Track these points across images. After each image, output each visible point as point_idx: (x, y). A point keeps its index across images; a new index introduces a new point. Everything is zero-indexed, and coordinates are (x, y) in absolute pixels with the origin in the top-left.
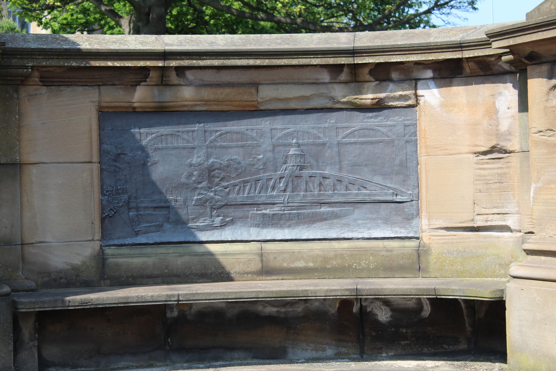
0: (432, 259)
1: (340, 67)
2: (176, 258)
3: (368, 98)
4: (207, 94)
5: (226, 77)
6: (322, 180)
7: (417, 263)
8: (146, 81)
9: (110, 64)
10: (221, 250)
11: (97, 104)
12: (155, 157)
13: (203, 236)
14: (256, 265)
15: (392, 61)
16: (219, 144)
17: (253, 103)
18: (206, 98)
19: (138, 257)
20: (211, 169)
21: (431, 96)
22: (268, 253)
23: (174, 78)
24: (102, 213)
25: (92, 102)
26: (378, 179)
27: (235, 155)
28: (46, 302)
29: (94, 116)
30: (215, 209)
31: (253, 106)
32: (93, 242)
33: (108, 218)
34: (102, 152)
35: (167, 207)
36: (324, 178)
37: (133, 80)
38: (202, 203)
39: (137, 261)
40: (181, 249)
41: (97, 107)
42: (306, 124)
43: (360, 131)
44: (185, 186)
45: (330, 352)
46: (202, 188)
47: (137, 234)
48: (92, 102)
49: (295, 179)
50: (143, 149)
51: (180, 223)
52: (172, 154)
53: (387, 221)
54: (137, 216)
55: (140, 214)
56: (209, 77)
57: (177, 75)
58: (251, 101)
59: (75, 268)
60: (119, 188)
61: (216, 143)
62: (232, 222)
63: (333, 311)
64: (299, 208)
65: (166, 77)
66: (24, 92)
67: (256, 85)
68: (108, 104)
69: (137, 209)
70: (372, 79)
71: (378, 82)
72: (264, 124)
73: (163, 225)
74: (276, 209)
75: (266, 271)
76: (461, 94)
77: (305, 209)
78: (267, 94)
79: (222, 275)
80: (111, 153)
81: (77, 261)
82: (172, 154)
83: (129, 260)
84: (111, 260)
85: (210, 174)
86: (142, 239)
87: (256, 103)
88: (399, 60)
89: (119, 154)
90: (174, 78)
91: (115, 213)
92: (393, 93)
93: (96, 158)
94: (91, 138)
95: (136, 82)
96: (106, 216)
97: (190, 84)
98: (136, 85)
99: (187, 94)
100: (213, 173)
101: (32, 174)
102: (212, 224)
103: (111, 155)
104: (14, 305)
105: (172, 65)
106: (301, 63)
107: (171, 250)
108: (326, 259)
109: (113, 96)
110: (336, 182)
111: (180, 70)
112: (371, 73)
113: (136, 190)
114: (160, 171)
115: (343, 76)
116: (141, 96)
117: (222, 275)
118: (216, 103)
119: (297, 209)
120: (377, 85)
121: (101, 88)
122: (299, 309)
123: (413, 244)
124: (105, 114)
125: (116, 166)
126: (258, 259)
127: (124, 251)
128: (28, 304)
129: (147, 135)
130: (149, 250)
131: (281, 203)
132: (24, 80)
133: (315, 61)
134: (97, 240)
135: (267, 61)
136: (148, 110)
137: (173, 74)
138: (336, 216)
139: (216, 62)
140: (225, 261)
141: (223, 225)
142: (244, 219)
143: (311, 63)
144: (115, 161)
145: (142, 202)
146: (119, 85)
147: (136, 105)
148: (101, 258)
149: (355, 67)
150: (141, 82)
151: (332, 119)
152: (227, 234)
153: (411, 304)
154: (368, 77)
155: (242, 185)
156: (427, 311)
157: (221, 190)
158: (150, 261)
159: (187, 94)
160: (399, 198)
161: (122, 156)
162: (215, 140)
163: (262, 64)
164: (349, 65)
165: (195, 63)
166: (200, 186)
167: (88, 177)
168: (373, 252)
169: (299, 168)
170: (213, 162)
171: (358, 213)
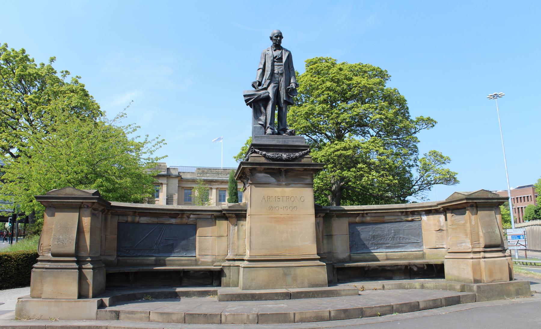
0: (426, 256)
1: (403, 212)
2: (367, 256)
3: (410, 219)
4: (372, 219)
5: (377, 215)
7: (423, 256)
12: (361, 233)
13: (373, 251)
14: (385, 258)
20: (374, 236)
21: (424, 218)
23: (365, 215)
26: (413, 237)
27: (379, 232)
28: (340, 265)
29: (348, 224)
33: (351, 247)
34: (349, 232)
35: (364, 244)
38: (372, 244)
39: (358, 257)
40: (368, 254)
42: (396, 225)
44: (368, 240)
45: (403, 278)
50: (358, 231)
51: (367, 248)
52: (365, 232)
53: (415, 247)
56: (373, 215)
59: (344, 258)
63: (403, 268)
66: (333, 219)
67: (384, 216)
72: (386, 225)
74: (389, 245)
75: (387, 259)
76: (431, 217)
78: (387, 218)
79: (378, 260)
81: (345, 257)
82: (365, 232)
85: (374, 237)
86: (359, 252)
90: (365, 215)
92: (416, 217)
99: (368, 219)
101: (335, 237)
104: (333, 266)
107: (366, 254)
108: (401, 256)
109: (352, 220)
111: (367, 214)
114: (362, 237)
115: (404, 214)
116: (358, 219)
117: (378, 260)
122: (396, 268)
123: (422, 252)
124: (350, 224)
128: (336, 266)
129: (359, 228)
132: (333, 216)
138: (403, 246)
140: (378, 257)
141: (377, 249)
142: (382, 247)
148: (350, 256)
149: (407, 212)
151: (402, 224)
152: (378, 251)
153: (422, 266)
156: (426, 268)
158: (361, 257)
159: (368, 219)
167: (347, 238)
168: (413, 254)
171: (408, 245)
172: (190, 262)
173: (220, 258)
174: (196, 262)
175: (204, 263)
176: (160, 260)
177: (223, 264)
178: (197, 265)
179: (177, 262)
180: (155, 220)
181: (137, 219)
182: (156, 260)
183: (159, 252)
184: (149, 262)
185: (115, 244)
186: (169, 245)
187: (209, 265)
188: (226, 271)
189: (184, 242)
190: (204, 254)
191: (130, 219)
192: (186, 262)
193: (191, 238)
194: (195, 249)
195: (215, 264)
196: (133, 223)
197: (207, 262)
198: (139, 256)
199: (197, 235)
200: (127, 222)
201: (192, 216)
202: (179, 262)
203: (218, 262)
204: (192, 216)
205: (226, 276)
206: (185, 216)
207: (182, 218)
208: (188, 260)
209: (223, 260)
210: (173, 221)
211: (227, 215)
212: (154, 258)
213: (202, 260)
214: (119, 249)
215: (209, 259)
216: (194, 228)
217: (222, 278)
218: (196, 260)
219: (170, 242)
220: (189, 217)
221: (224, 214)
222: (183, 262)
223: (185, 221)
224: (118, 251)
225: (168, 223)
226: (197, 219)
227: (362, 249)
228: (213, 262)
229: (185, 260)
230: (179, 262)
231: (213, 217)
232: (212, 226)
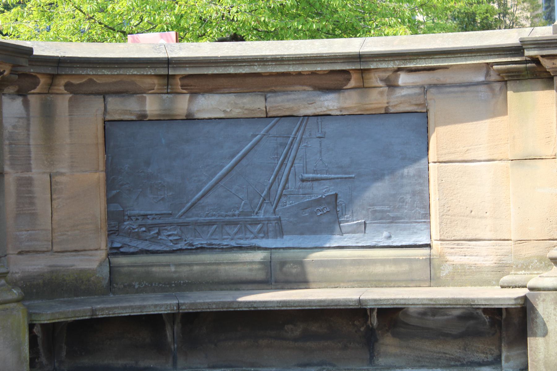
172: (405, 267)
173: (530, 251)
174: (431, 274)
175: (462, 275)
176: (283, 263)
177: (534, 282)
178: (432, 280)
179: (353, 271)
180: (254, 104)
181: (182, 104)
182: (267, 264)
183: (280, 232)
184: (242, 271)
185: (98, 207)
186: (319, 202)
187: (487, 283)
188: (544, 308)
189: (378, 190)
190: (461, 233)
191: (152, 106)
192: (389, 269)
193: (410, 170)
194: (427, 215)
195: (506, 279)
196: (167, 119)
197: (478, 269)
198: (202, 249)
199: (432, 155)
200: (142, 118)
201: (403, 79)
202: (362, 270)
203: (518, 268)
204: (403, 79)
205: (545, 334)
206: (375, 80)
207: (363, 87)
208: (396, 261)
209: (541, 259)
210: (330, 103)
211: (547, 64)
212: (259, 256)
213: (456, 259)
214: (115, 223)
215: (483, 256)
216: (419, 123)
217: (531, 341)
218: (430, 260)
219: (323, 190)
220: (392, 85)
221: (535, 60)
222: (379, 269)
223: (377, 99)
224: (112, 233)
225: (310, 111)
226: (425, 89)
228: (502, 268)
229: (384, 262)
230: (362, 270)
231: (494, 77)
232: (494, 114)
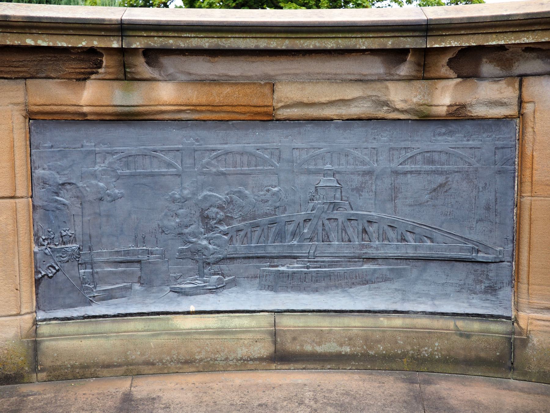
6: (366, 225)
8: (97, 73)
9: (30, 42)
10: (216, 326)
11: (22, 107)
14: (264, 349)
15: (490, 43)
16: (214, 170)
17: (265, 109)
18: (194, 101)
19: (90, 338)
22: (284, 331)
23: (143, 68)
24: (37, 272)
25: (15, 104)
30: (209, 264)
31: (266, 114)
32: (19, 317)
36: (369, 222)
37: (77, 70)
40: (156, 324)
41: (24, 113)
43: (426, 154)
46: (190, 234)
47: (89, 303)
48: (15, 104)
49: (327, 222)
54: (92, 274)
55: (97, 273)
57: (148, 63)
58: (264, 106)
60: (64, 234)
61: (211, 168)
62: (234, 283)
64: (331, 264)
65: (130, 68)
68: (40, 108)
69: (92, 264)
70: (451, 73)
71: (459, 80)
73: (131, 288)
74: (295, 266)
77: (340, 266)
80: (51, 183)
83: (76, 343)
84: (48, 345)
87: (271, 109)
88: (502, 42)
89: (63, 184)
91: (58, 271)
93: (22, 190)
94: (13, 161)
95: (83, 73)
96: (43, 276)
97: (170, 78)
98: (85, 79)
100: (206, 212)
102: (205, 286)
103: (50, 186)
105: (134, 46)
106: (341, 47)
110: (386, 227)
112: (450, 63)
113: (90, 238)
115: (404, 70)
118: (210, 108)
119: (329, 266)
120: (457, 84)
121: (29, 82)
125: (56, 201)
126: (269, 339)
127: (70, 328)
130: (107, 326)
131: (305, 257)
133: (364, 44)
134: (28, 313)
135: (287, 42)
136: (108, 118)
137: (141, 60)
139: (206, 43)
143: (358, 47)
144: (57, 194)
145: (100, 254)
146: (58, 78)
147: (85, 109)
150: (92, 73)
154: (445, 71)
155: (249, 230)
157: (217, 238)
160: (481, 256)
161: (68, 187)
162: (208, 163)
163: (279, 48)
164: (416, 51)
165: (171, 43)
166: (186, 231)
169: (332, 206)
170: (205, 198)
227: (125, 292)
